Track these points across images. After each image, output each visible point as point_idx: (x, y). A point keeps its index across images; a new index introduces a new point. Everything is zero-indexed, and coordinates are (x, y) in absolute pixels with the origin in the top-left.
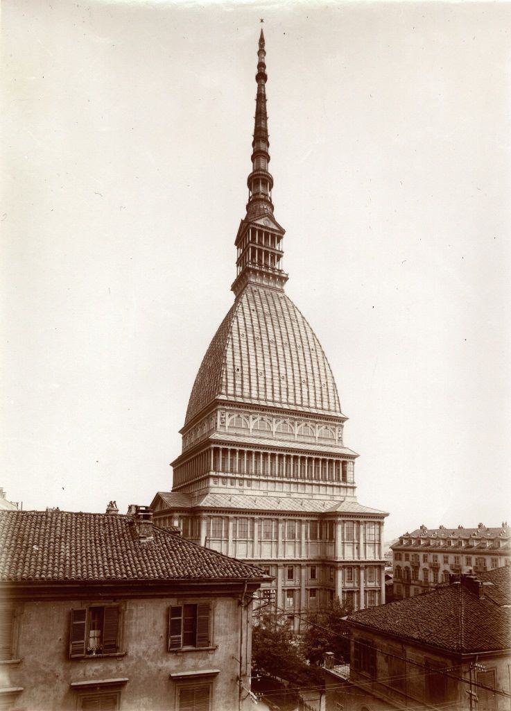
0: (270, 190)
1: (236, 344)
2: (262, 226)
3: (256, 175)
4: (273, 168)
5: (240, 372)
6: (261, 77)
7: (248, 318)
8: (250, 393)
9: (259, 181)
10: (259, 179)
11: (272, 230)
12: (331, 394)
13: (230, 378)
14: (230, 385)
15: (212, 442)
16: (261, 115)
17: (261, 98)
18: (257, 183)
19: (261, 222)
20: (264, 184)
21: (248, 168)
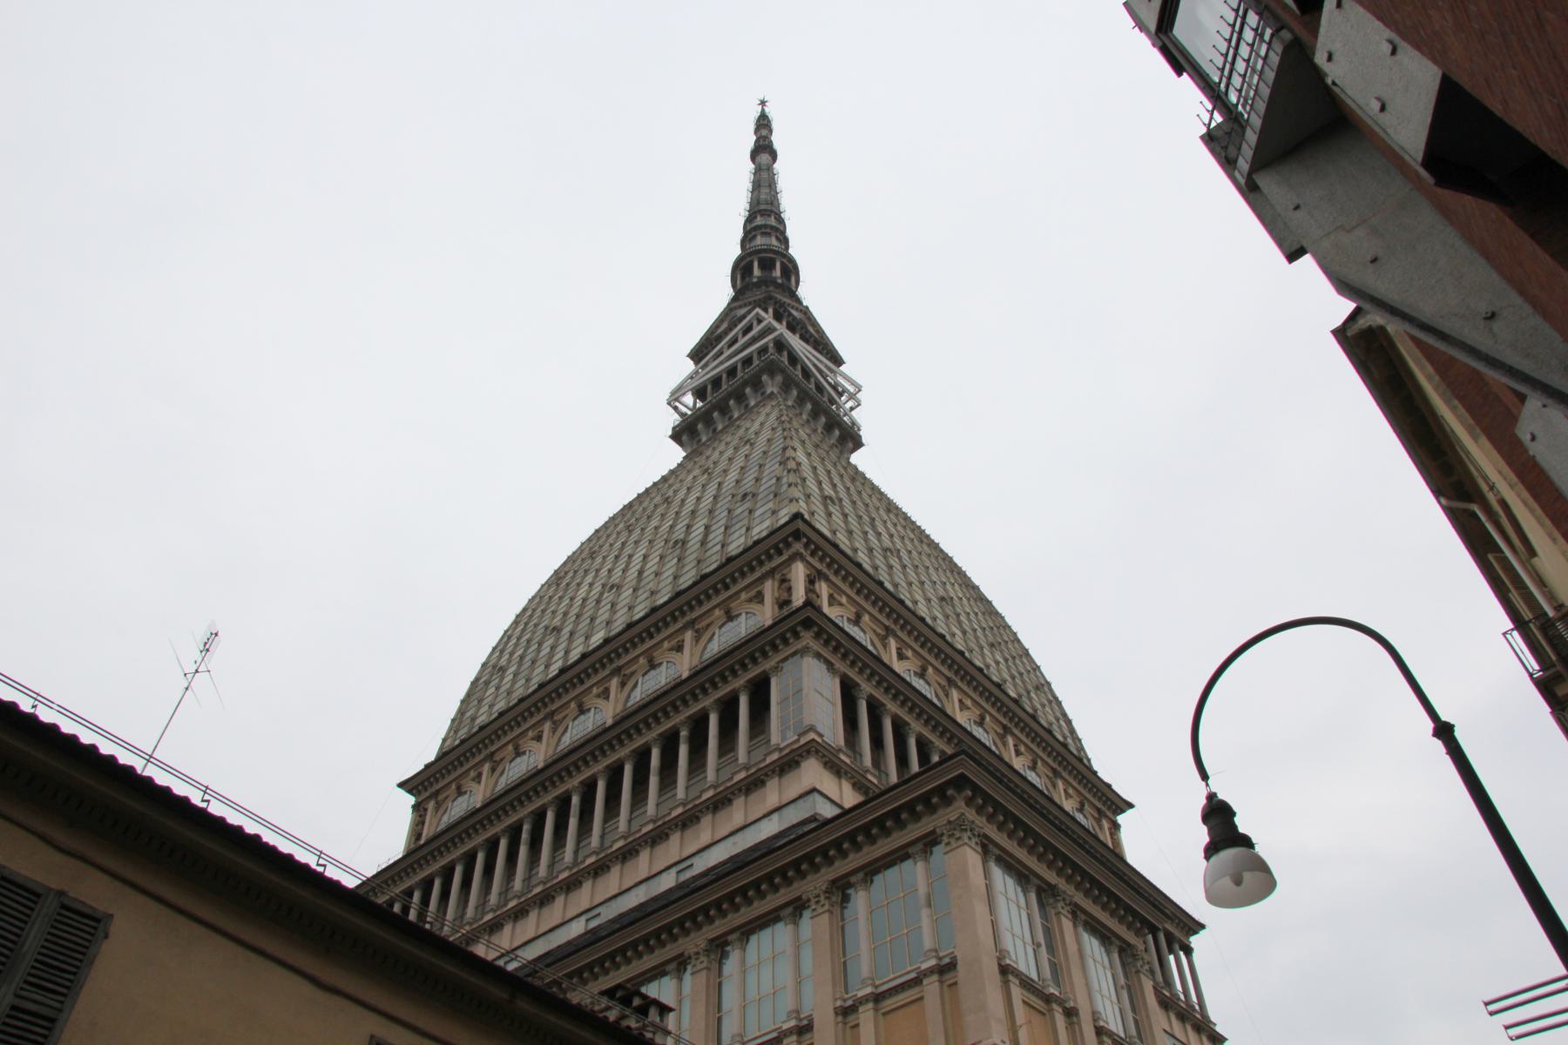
2: (794, 318)
6: (763, 150)
18: (767, 265)
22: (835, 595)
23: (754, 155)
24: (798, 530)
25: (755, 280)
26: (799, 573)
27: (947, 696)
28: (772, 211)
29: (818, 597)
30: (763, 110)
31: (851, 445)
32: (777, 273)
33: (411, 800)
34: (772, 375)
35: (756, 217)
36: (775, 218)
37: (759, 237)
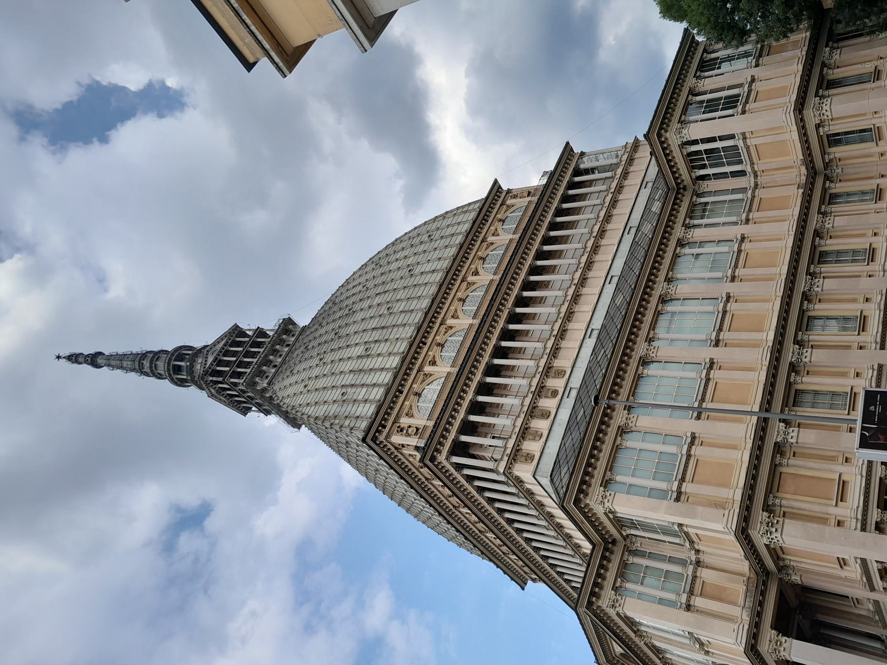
2: (214, 361)
3: (169, 370)
5: (349, 390)
6: (94, 360)
10: (174, 366)
11: (225, 346)
12: (448, 221)
13: (349, 409)
15: (433, 459)
18: (178, 369)
19: (210, 359)
22: (406, 411)
23: (97, 366)
24: (372, 440)
25: (189, 378)
26: (397, 439)
27: (451, 327)
28: (139, 363)
29: (410, 427)
30: (64, 358)
33: (530, 582)
34: (255, 384)
35: (145, 372)
36: (143, 360)
37: (159, 372)
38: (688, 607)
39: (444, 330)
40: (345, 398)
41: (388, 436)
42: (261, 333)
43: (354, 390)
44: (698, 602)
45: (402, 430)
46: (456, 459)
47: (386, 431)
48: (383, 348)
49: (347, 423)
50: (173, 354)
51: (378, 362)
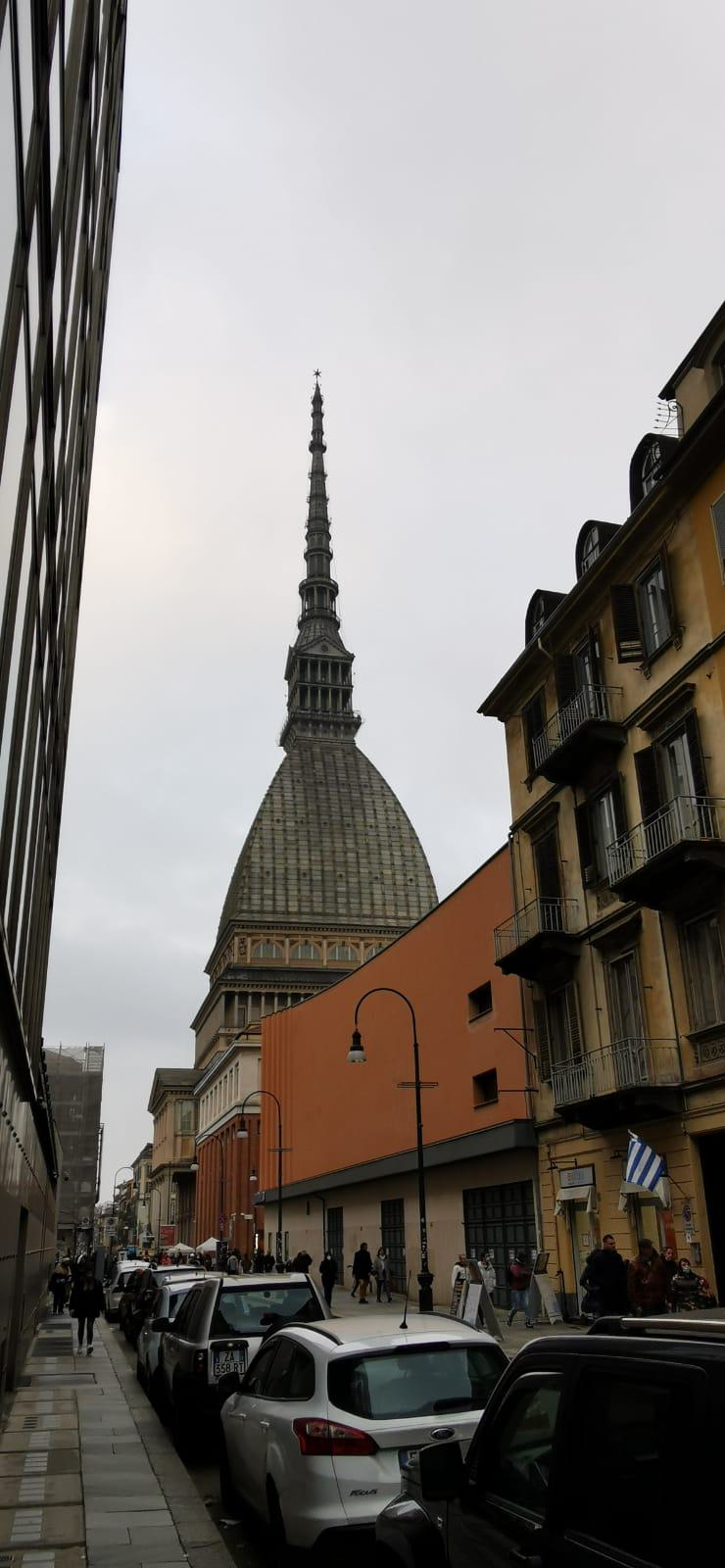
0: (333, 599)
1: (267, 836)
2: (317, 656)
4: (337, 572)
5: (271, 877)
6: (317, 447)
7: (288, 796)
8: (287, 906)
9: (319, 591)
10: (312, 590)
11: (332, 657)
14: (256, 897)
16: (318, 498)
17: (318, 475)
19: (316, 651)
20: (321, 591)
21: (300, 571)
31: (353, 728)
32: (316, 603)
38: (176, 1136)
39: (317, 940)
40: (265, 876)
41: (237, 934)
42: (347, 694)
43: (271, 881)
44: (179, 1140)
45: (242, 943)
46: (223, 997)
47: (239, 930)
48: (305, 889)
49: (246, 891)
50: (323, 583)
51: (293, 893)
